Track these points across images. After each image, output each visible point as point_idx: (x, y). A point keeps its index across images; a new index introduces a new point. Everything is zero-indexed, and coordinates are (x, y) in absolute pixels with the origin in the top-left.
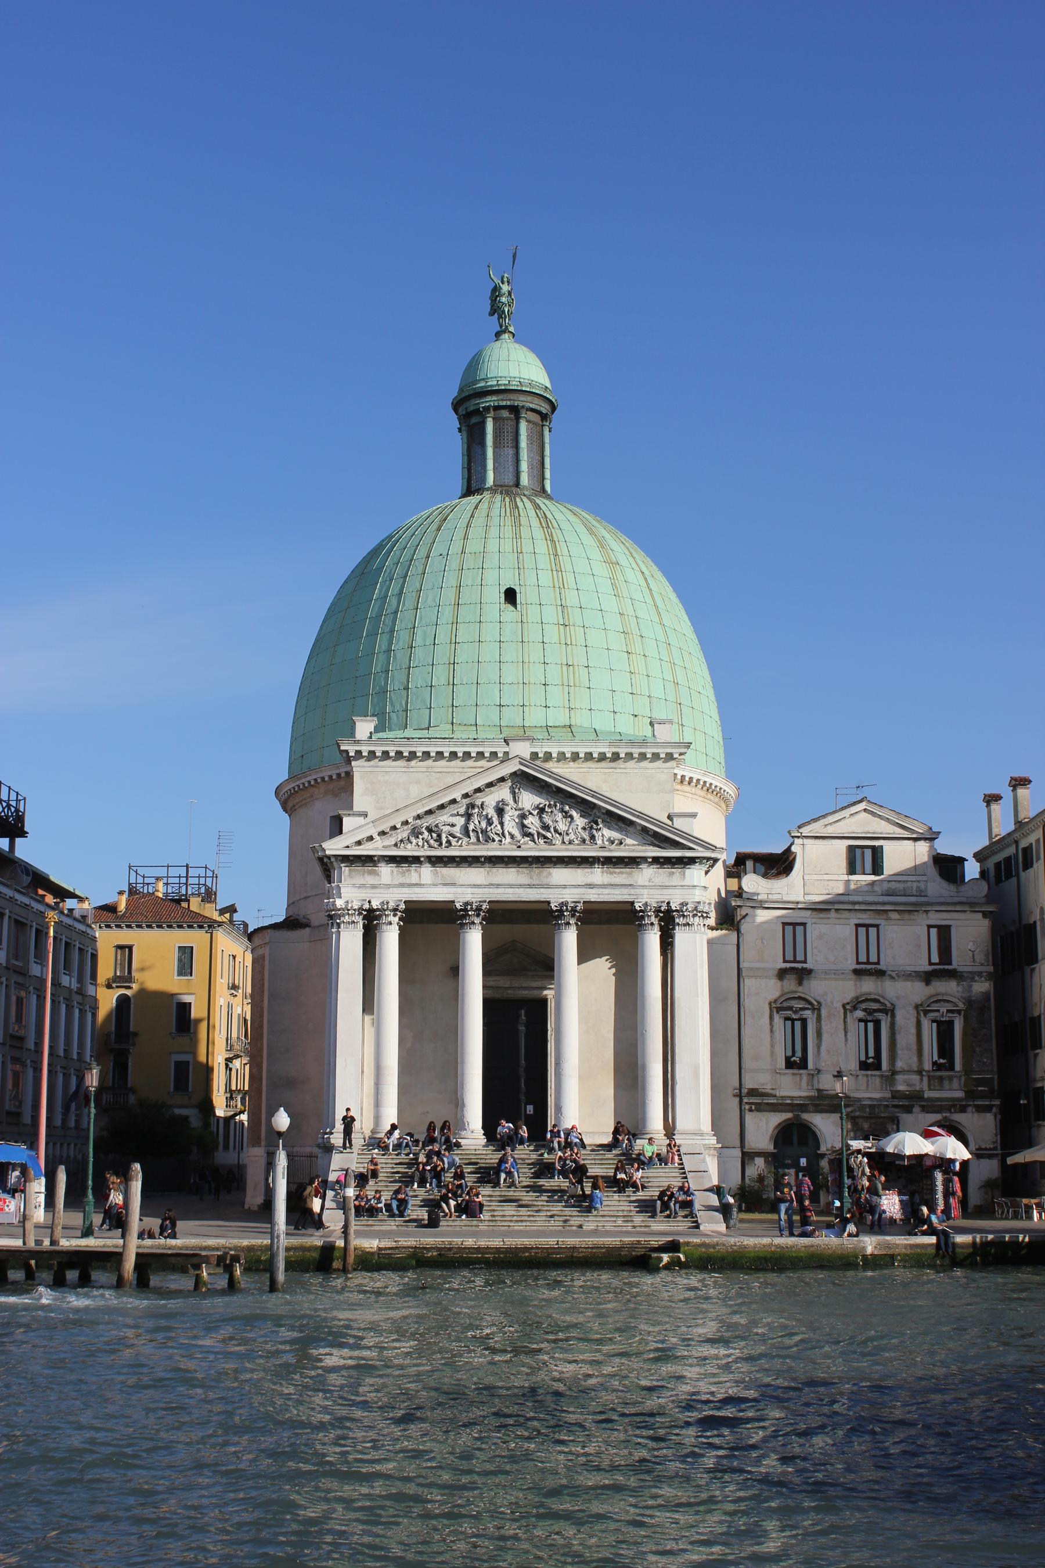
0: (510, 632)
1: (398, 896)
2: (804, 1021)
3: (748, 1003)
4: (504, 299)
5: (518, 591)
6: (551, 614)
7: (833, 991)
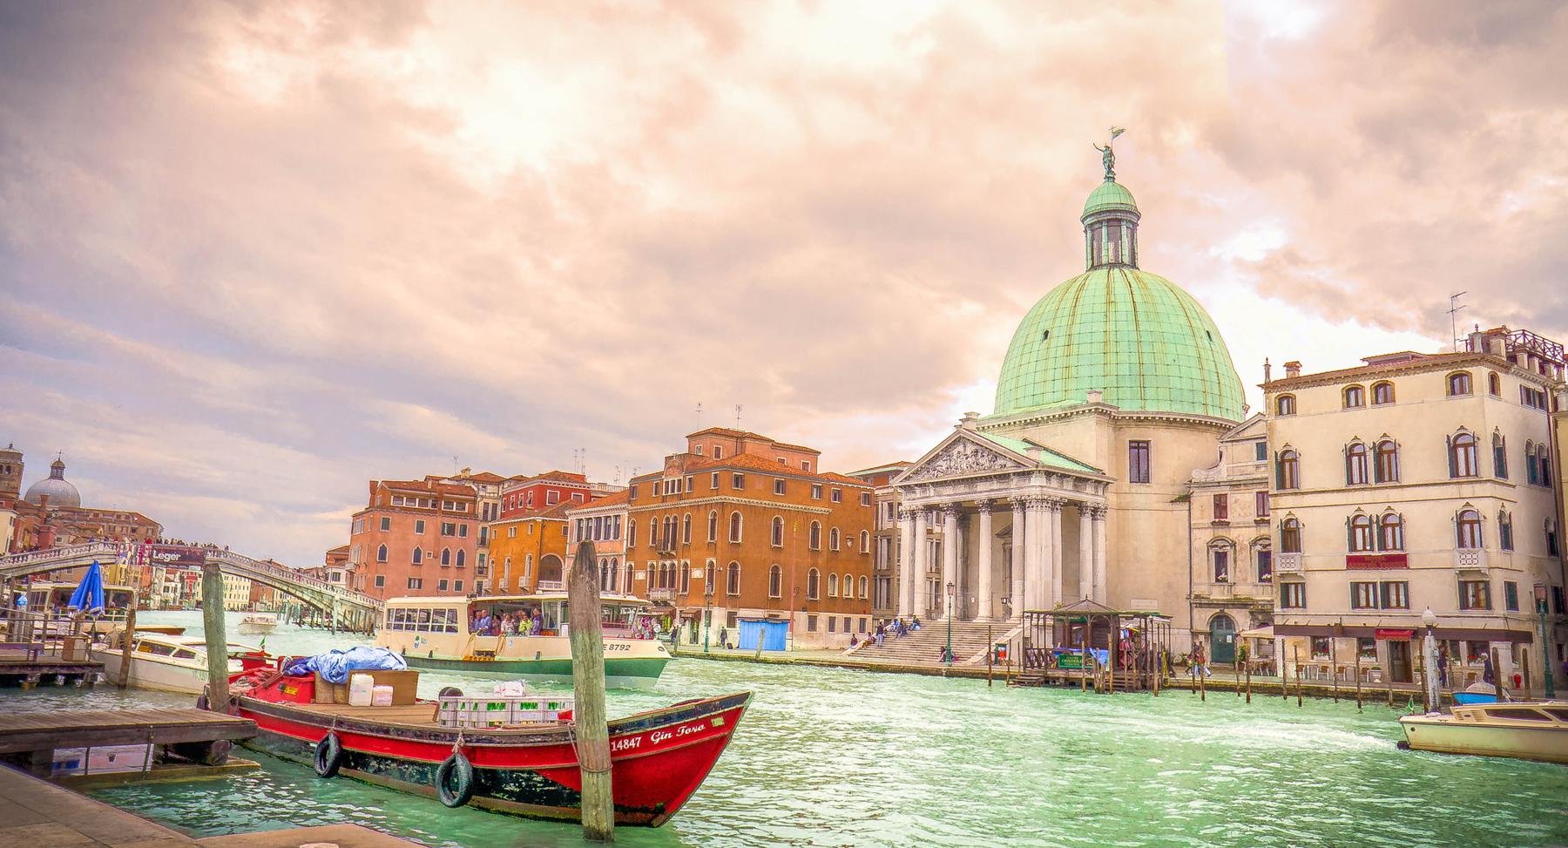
1: (920, 503)
2: (1225, 554)
3: (1196, 544)
6: (1062, 341)
7: (1243, 535)
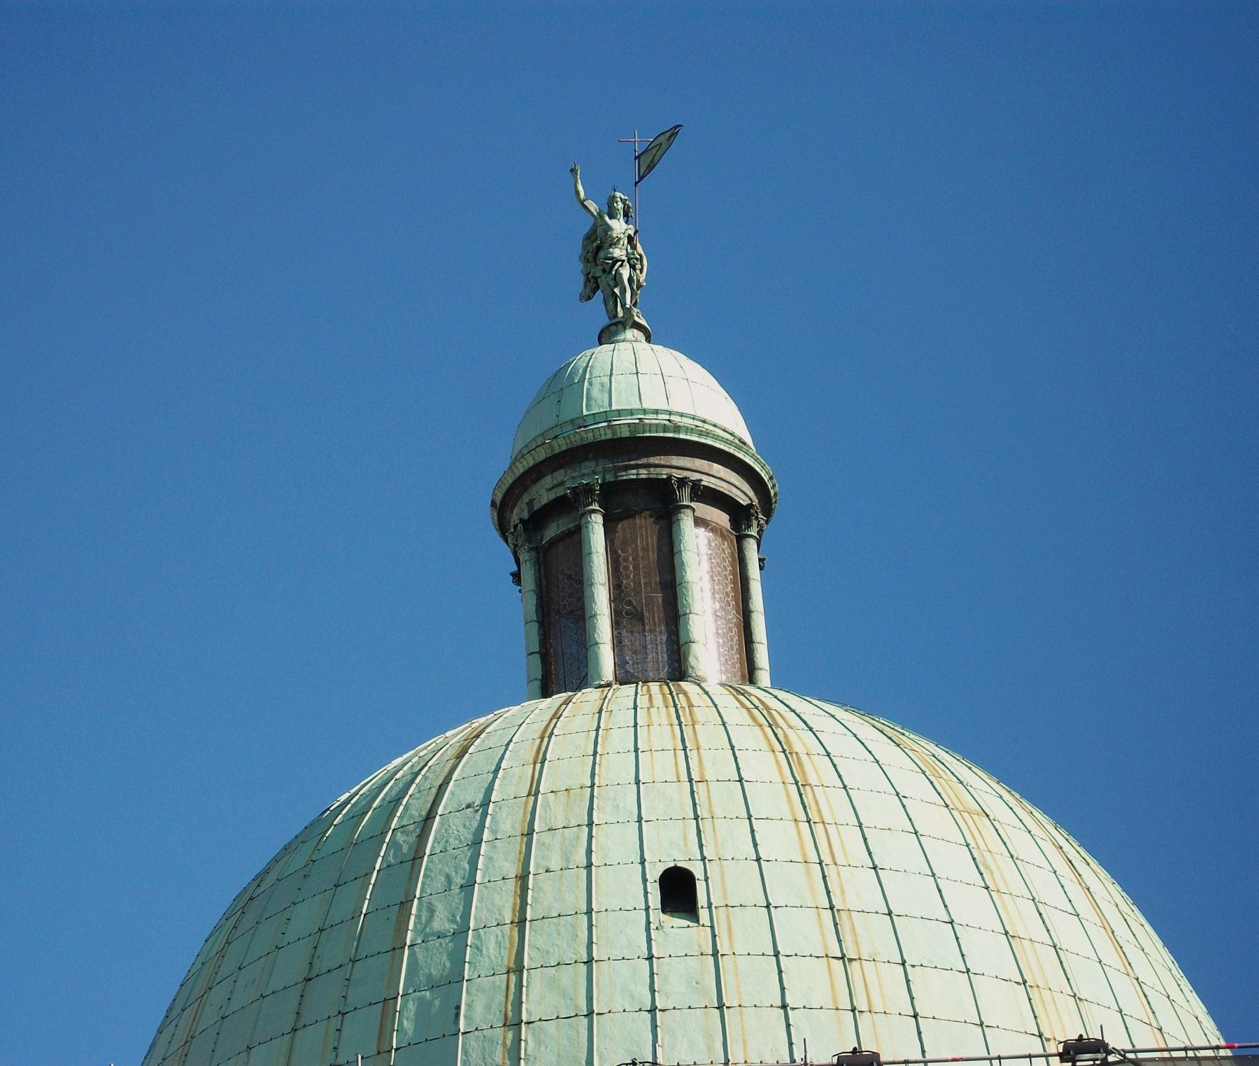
0: (683, 978)
4: (617, 253)
5: (698, 873)
6: (803, 931)
